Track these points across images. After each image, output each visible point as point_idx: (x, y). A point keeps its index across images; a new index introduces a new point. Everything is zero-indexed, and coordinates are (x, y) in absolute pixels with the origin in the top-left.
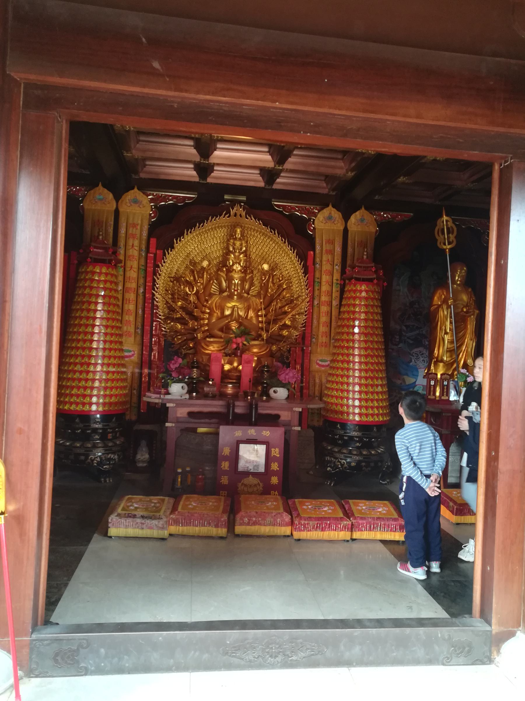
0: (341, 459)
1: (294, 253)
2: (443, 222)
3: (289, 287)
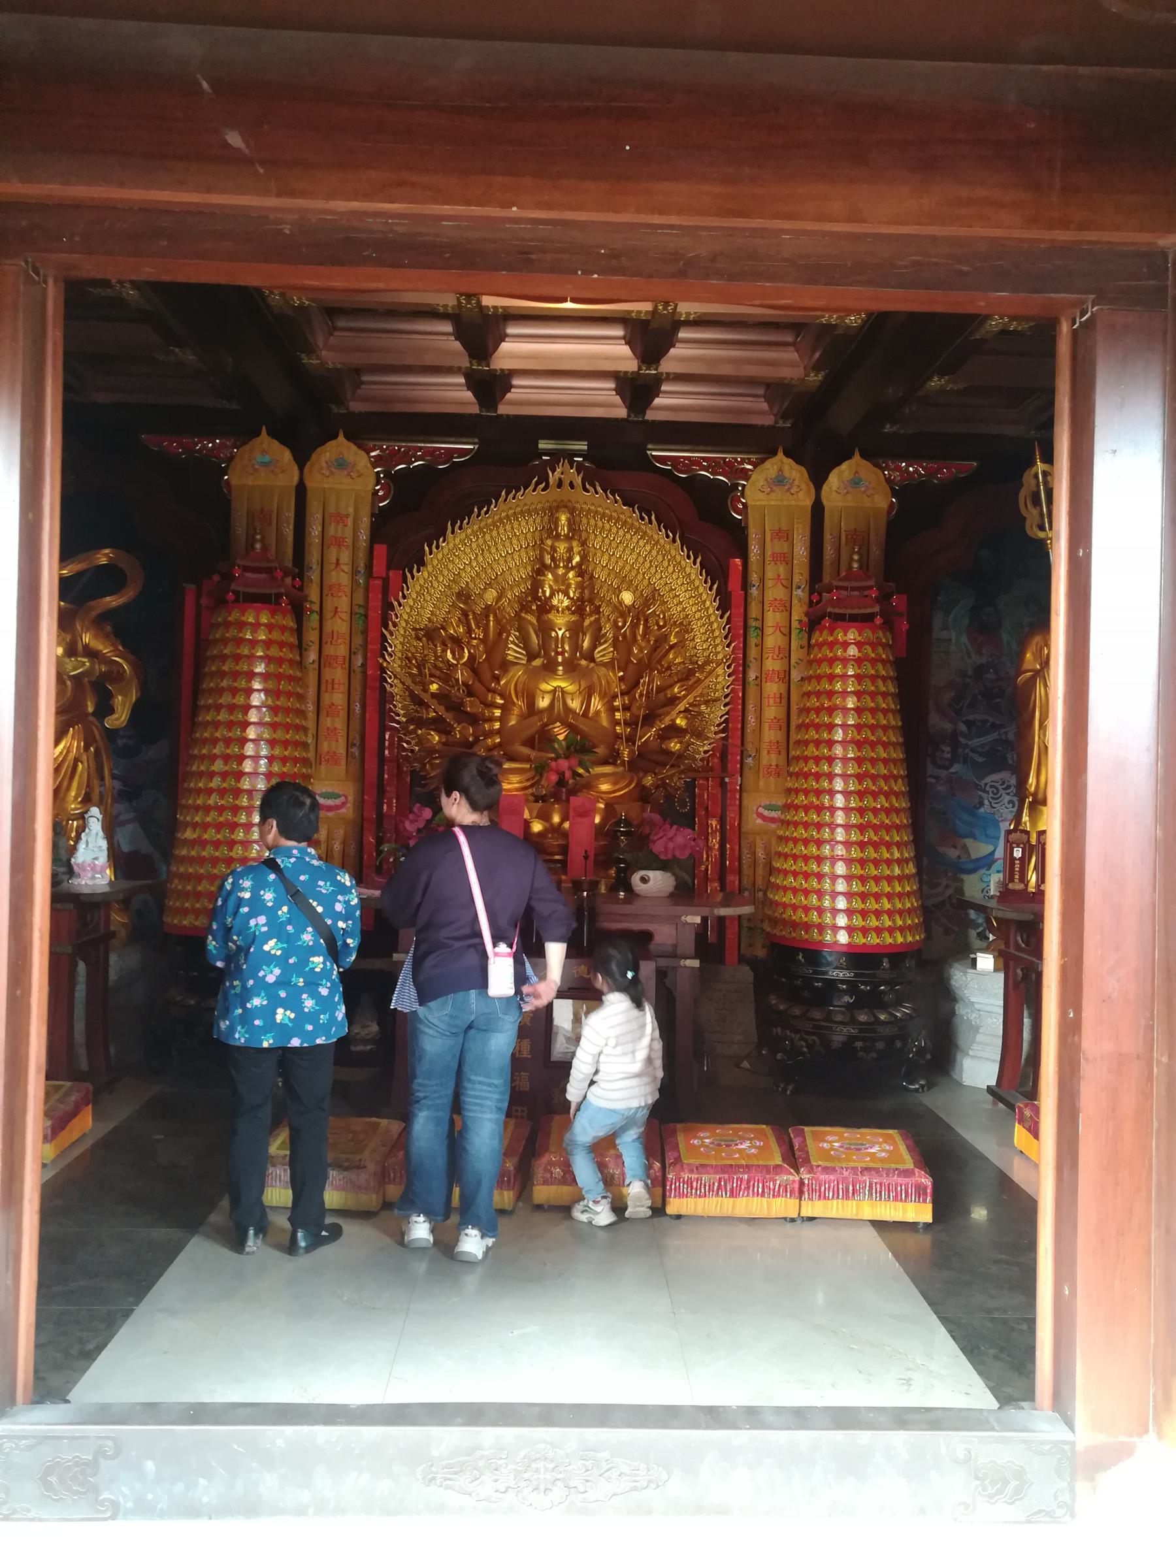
1: (695, 563)
2: (1036, 476)
3: (681, 643)
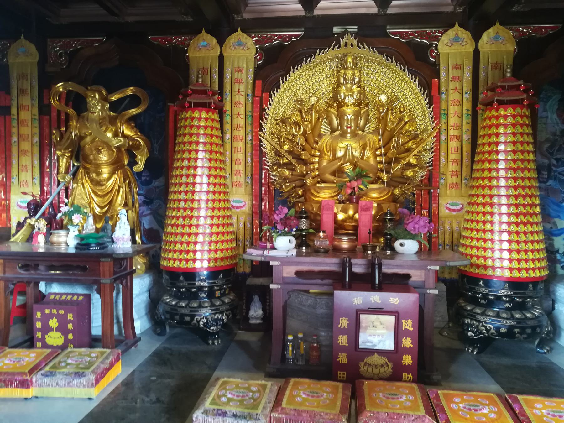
0: (486, 323)
3: (412, 120)
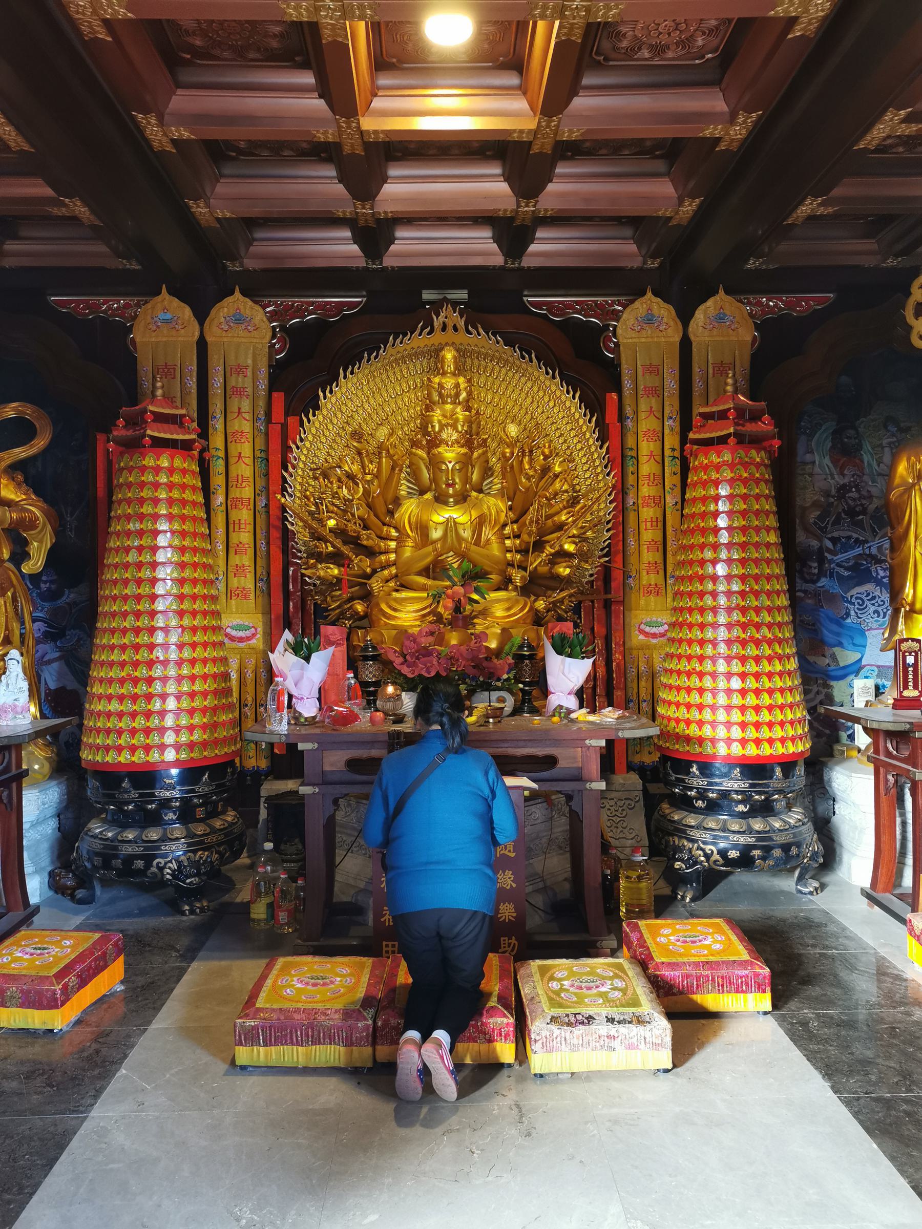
0: (705, 843)
1: (574, 398)
